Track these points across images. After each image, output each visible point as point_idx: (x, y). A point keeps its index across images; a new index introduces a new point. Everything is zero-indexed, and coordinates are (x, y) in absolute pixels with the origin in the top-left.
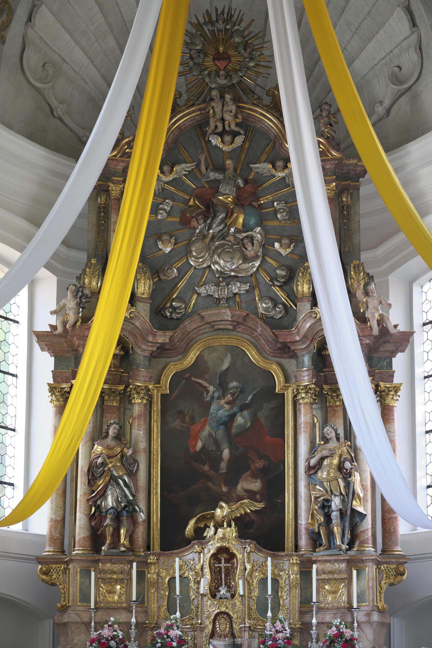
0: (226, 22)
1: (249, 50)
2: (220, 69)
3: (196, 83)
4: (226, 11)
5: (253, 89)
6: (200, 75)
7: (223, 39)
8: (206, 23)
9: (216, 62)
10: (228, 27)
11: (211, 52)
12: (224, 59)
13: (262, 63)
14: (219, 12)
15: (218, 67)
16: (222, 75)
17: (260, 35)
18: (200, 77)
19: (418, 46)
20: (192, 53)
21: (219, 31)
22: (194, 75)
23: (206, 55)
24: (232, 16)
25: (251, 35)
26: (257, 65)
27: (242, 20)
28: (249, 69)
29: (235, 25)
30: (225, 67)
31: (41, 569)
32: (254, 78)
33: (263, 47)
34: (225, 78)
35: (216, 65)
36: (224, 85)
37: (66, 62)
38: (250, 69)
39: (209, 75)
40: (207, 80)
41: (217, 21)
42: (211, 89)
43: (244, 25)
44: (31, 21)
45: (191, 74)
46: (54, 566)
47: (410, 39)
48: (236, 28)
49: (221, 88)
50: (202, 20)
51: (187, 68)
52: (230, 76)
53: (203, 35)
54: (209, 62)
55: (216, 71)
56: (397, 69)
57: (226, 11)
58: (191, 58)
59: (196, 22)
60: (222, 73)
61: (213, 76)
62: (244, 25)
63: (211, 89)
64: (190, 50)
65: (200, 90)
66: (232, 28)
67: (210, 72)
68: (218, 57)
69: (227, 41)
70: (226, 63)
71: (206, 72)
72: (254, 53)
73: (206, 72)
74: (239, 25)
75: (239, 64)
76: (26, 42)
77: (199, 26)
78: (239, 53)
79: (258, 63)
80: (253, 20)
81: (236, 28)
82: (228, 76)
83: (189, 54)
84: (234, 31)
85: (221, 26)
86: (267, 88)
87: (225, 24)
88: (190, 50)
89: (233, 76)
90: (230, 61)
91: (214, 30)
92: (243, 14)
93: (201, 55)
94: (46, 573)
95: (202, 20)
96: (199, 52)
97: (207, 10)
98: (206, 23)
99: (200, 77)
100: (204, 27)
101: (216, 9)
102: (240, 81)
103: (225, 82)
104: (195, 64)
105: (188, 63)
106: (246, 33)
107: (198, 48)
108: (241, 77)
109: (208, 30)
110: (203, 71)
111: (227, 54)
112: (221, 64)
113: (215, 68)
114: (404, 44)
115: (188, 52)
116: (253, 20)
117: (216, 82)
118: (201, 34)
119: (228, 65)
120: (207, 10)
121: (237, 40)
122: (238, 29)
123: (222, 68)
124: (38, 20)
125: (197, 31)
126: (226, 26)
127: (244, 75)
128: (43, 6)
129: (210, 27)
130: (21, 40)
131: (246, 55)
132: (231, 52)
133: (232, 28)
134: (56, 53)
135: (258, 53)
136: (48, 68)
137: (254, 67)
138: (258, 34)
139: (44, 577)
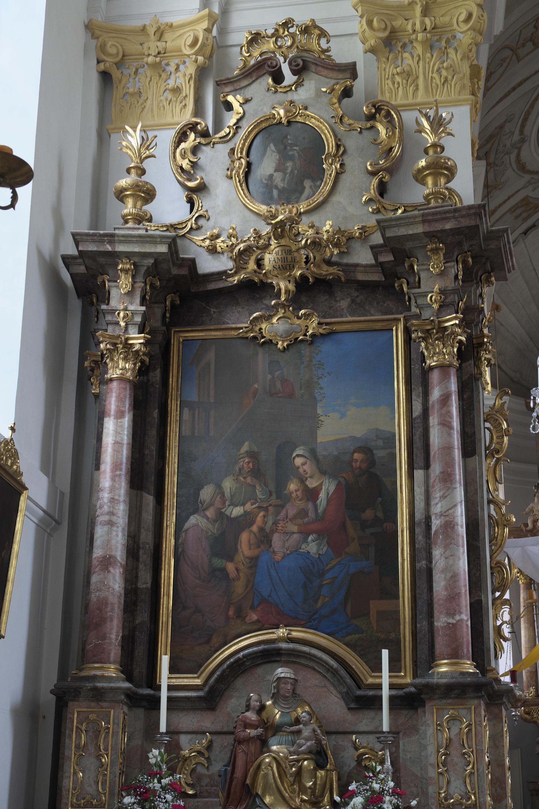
31: (524, 710)
46: (534, 708)
94: (528, 713)
139: (526, 716)
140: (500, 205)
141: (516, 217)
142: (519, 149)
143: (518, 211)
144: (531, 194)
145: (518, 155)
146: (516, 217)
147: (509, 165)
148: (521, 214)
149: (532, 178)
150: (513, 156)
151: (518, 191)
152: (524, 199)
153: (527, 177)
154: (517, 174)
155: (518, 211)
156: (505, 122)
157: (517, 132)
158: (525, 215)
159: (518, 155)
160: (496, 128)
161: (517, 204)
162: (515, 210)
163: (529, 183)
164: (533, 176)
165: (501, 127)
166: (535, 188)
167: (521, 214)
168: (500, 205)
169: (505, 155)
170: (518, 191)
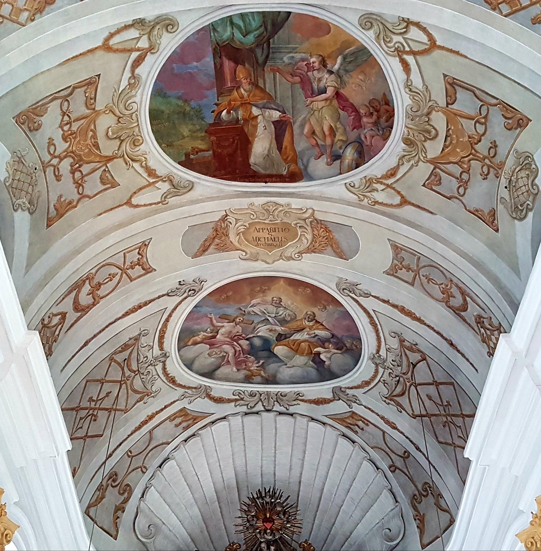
0: (272, 497)
1: (287, 516)
2: (268, 529)
3: (251, 538)
4: (271, 490)
5: (290, 543)
6: (254, 532)
7: (269, 508)
8: (258, 498)
9: (265, 524)
10: (273, 500)
11: (261, 517)
12: (270, 522)
13: (296, 525)
14: (267, 491)
15: (266, 527)
16: (269, 533)
17: (294, 506)
18: (254, 534)
19: (400, 515)
20: (249, 517)
21: (267, 503)
22: (249, 533)
23: (258, 519)
24: (275, 493)
25: (288, 506)
26: (292, 526)
27: (281, 496)
28: (287, 528)
29: (277, 499)
30: (271, 527)
32: (291, 535)
33: (296, 514)
34: (270, 536)
35: (264, 525)
36: (270, 540)
37: (164, 524)
38: (287, 528)
39: (260, 533)
40: (258, 536)
41: (265, 497)
42: (261, 542)
43: (283, 499)
44: (143, 497)
45: (248, 532)
47: (394, 511)
48: (278, 501)
49: (268, 542)
50: (255, 496)
51: (245, 528)
52: (274, 534)
53: (256, 505)
54: (260, 524)
55: (264, 530)
56: (387, 530)
57: (271, 490)
58: (248, 521)
59: (252, 497)
60: (268, 531)
61: (262, 534)
62: (283, 499)
63: (261, 542)
64: (248, 515)
65: (253, 543)
66: (275, 501)
67: (260, 530)
68: (266, 520)
69: (272, 510)
70: (271, 524)
71: (258, 531)
72: (290, 518)
73: (258, 531)
74: (280, 499)
75: (280, 525)
76: (139, 511)
77: (253, 500)
78: (280, 518)
79: (293, 525)
80: (289, 496)
81: (278, 501)
82: (272, 533)
83: (247, 518)
84: (277, 503)
85: (268, 499)
86: (299, 543)
87: (270, 498)
88: (248, 515)
89: (276, 534)
90: (274, 523)
91: (263, 503)
92: (282, 492)
93: (255, 519)
95: (255, 496)
96: (253, 516)
97: (259, 489)
98: (258, 498)
99: (254, 534)
100: (257, 500)
101: (265, 489)
102: (281, 537)
103: (270, 537)
104: (250, 525)
105: (246, 524)
106: (284, 504)
107: (253, 514)
108: (282, 534)
109: (260, 502)
110: (256, 530)
111: (272, 518)
112: (269, 525)
113: (263, 528)
114: (391, 514)
115: (246, 517)
116: (289, 496)
117: (264, 538)
118: (255, 505)
119: (272, 526)
120: (259, 489)
121: (279, 509)
122: (279, 502)
123: (269, 528)
124: (148, 496)
125: (252, 503)
126: (271, 500)
127: (283, 533)
128: (153, 487)
129: (260, 500)
130: (136, 509)
131: (285, 519)
132: (275, 517)
133: (275, 501)
134: (158, 518)
135: (293, 518)
136: (152, 528)
137: (290, 527)
138: (292, 505)
140: (157, 413)
141: (177, 426)
142: (164, 363)
143: (178, 420)
144: (188, 406)
145: (164, 369)
146: (177, 426)
147: (157, 376)
148: (180, 424)
149: (185, 392)
150: (159, 368)
151: (174, 402)
152: (181, 410)
153: (181, 391)
154: (168, 385)
155: (178, 420)
156: (140, 335)
157: (156, 346)
158: (184, 424)
159: (164, 369)
160: (130, 339)
161: (175, 414)
162: (174, 419)
163: (183, 396)
164: (187, 391)
165: (137, 339)
166: (191, 402)
167: (180, 424)
168: (157, 413)
169: (149, 365)
170: (174, 402)
